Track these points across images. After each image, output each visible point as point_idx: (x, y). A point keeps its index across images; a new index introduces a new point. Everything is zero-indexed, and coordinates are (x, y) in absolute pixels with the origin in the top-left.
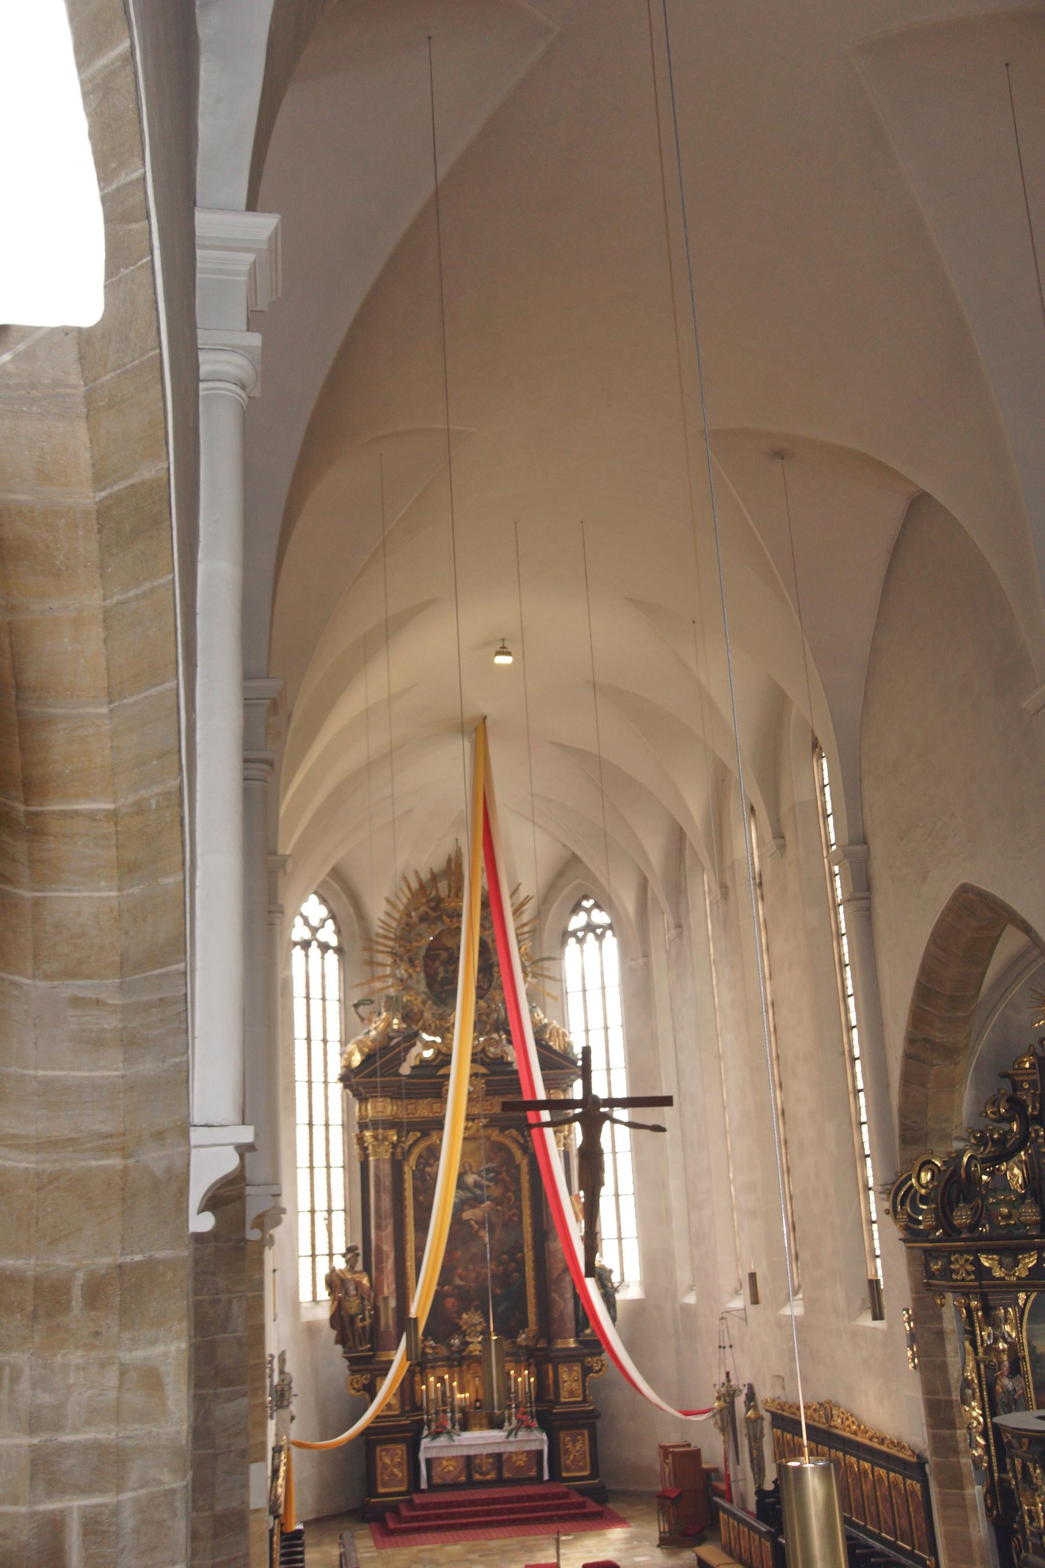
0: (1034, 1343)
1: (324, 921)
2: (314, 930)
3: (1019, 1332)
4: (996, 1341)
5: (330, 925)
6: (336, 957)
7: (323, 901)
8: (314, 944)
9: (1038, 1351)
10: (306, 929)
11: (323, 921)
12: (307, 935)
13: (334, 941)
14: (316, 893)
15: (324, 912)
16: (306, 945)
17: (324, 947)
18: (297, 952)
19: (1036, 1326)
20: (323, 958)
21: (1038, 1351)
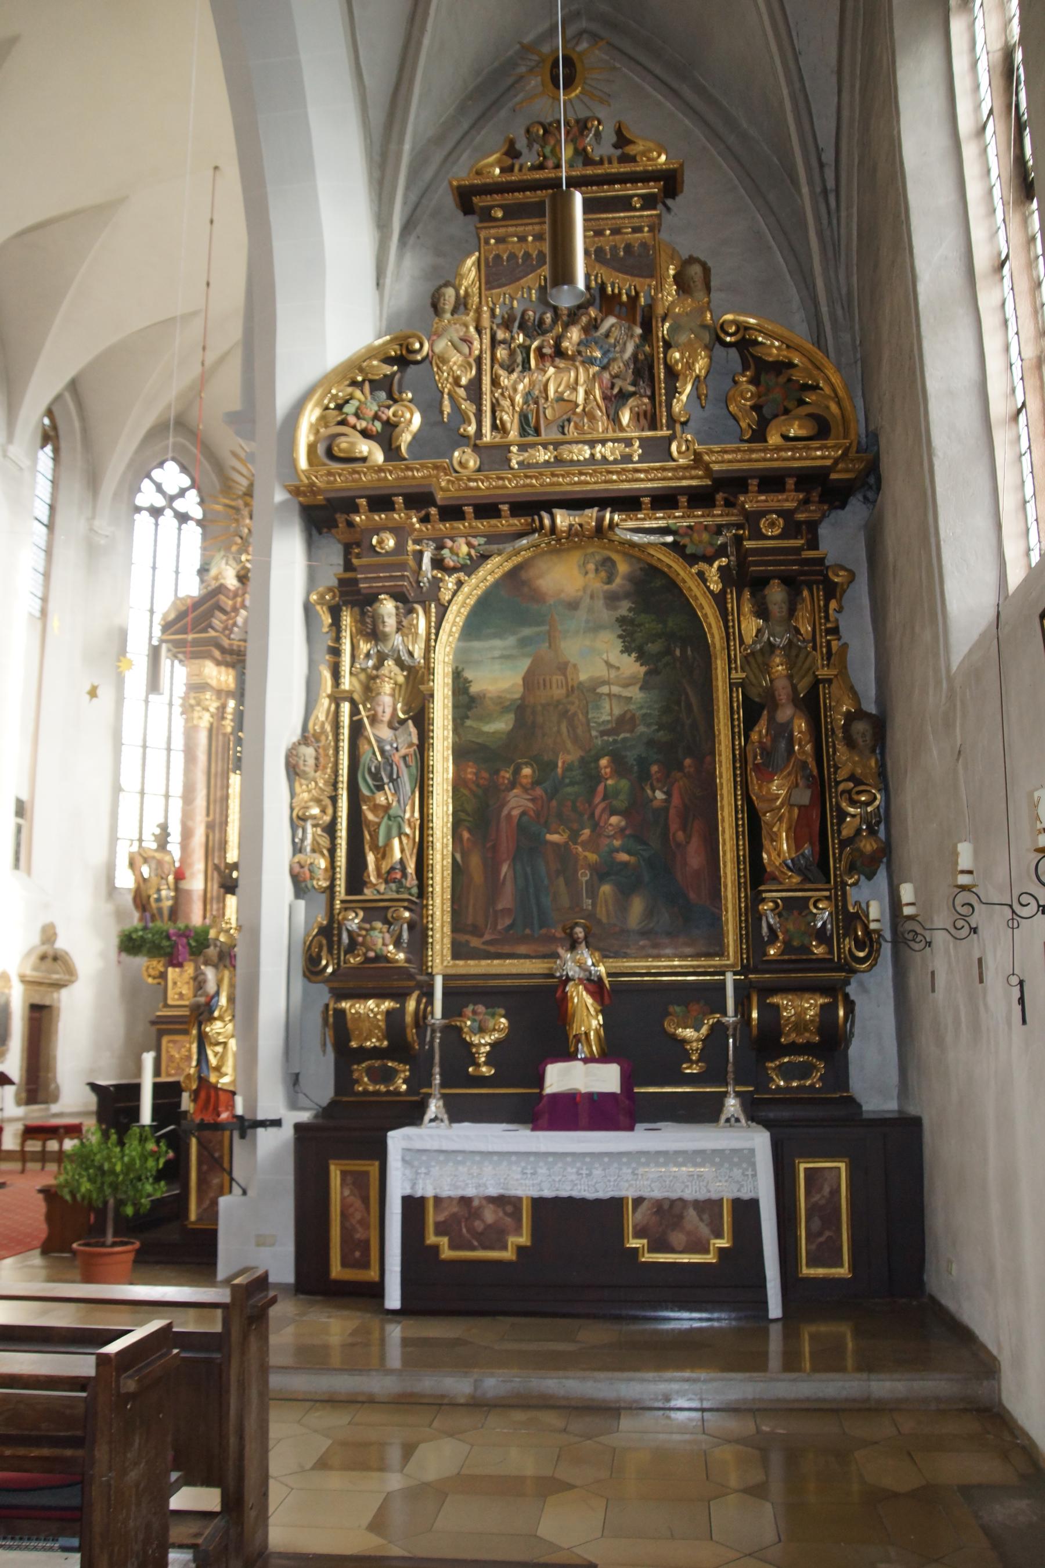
0: (468, 674)
1: (182, 493)
2: (171, 499)
3: (428, 650)
4: (379, 665)
5: (193, 495)
6: (199, 530)
7: (184, 469)
8: (168, 513)
9: (474, 689)
10: (160, 496)
11: (182, 493)
12: (160, 502)
13: (197, 513)
14: (173, 459)
15: (185, 481)
16: (156, 512)
17: (183, 518)
18: (143, 519)
19: (476, 644)
20: (180, 529)
21: (474, 689)
